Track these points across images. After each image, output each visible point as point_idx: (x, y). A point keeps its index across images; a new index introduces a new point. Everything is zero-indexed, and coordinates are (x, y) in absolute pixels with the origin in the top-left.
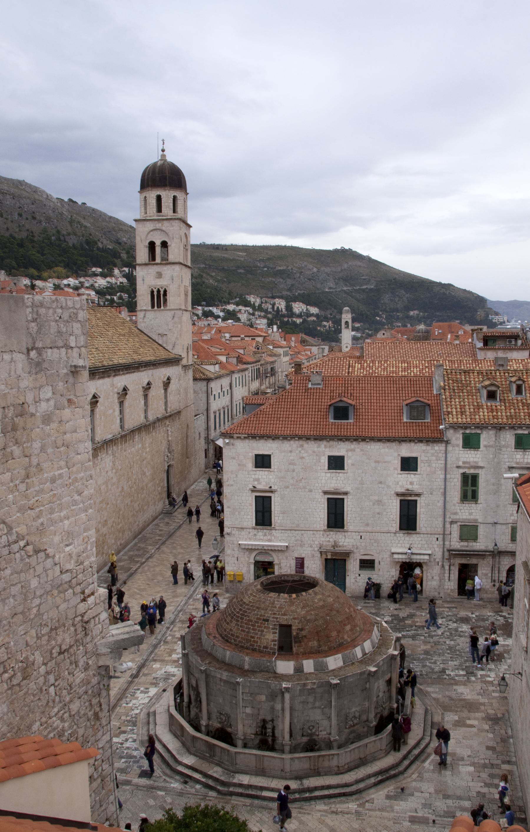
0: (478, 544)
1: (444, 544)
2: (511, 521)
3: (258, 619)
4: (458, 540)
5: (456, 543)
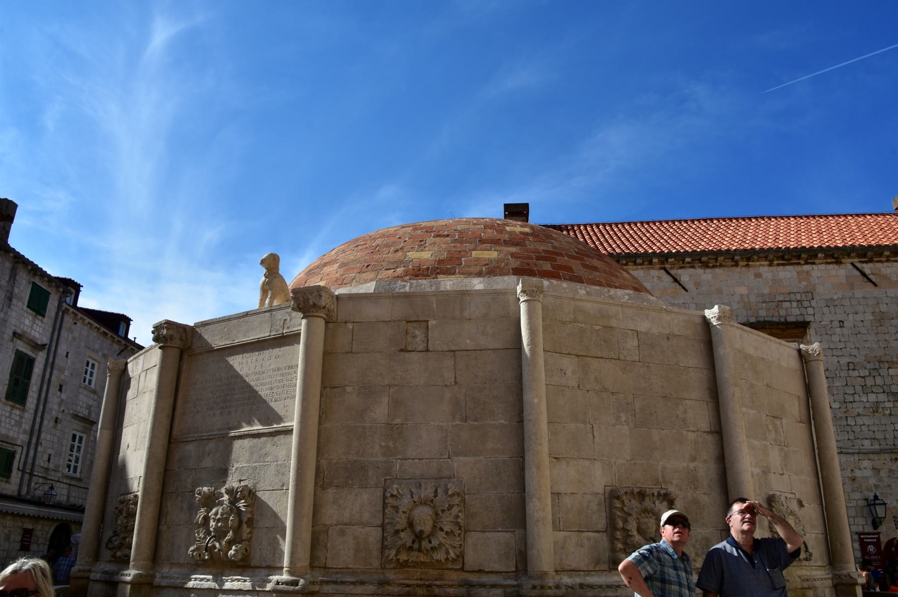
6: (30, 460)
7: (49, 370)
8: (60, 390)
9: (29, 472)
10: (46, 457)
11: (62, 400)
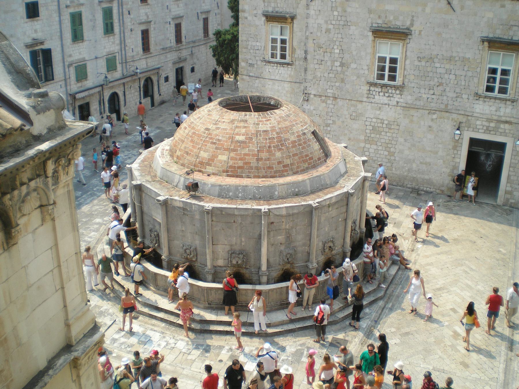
0: (88, 82)
1: (67, 90)
2: (105, 54)
3: (298, 136)
4: (76, 82)
5: (74, 87)
6: (124, 56)
7: (121, 7)
8: (129, 14)
9: (125, 62)
10: (131, 51)
11: (131, 18)
